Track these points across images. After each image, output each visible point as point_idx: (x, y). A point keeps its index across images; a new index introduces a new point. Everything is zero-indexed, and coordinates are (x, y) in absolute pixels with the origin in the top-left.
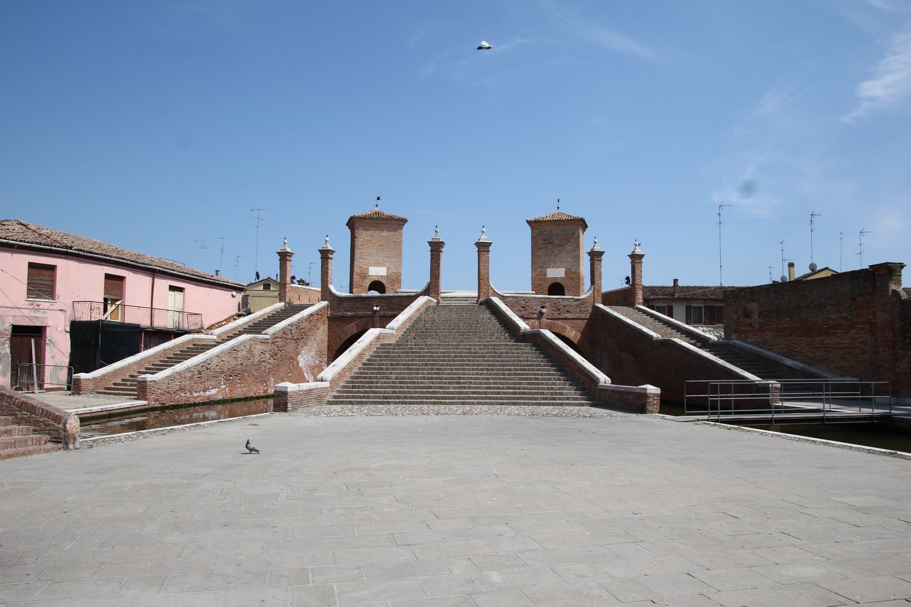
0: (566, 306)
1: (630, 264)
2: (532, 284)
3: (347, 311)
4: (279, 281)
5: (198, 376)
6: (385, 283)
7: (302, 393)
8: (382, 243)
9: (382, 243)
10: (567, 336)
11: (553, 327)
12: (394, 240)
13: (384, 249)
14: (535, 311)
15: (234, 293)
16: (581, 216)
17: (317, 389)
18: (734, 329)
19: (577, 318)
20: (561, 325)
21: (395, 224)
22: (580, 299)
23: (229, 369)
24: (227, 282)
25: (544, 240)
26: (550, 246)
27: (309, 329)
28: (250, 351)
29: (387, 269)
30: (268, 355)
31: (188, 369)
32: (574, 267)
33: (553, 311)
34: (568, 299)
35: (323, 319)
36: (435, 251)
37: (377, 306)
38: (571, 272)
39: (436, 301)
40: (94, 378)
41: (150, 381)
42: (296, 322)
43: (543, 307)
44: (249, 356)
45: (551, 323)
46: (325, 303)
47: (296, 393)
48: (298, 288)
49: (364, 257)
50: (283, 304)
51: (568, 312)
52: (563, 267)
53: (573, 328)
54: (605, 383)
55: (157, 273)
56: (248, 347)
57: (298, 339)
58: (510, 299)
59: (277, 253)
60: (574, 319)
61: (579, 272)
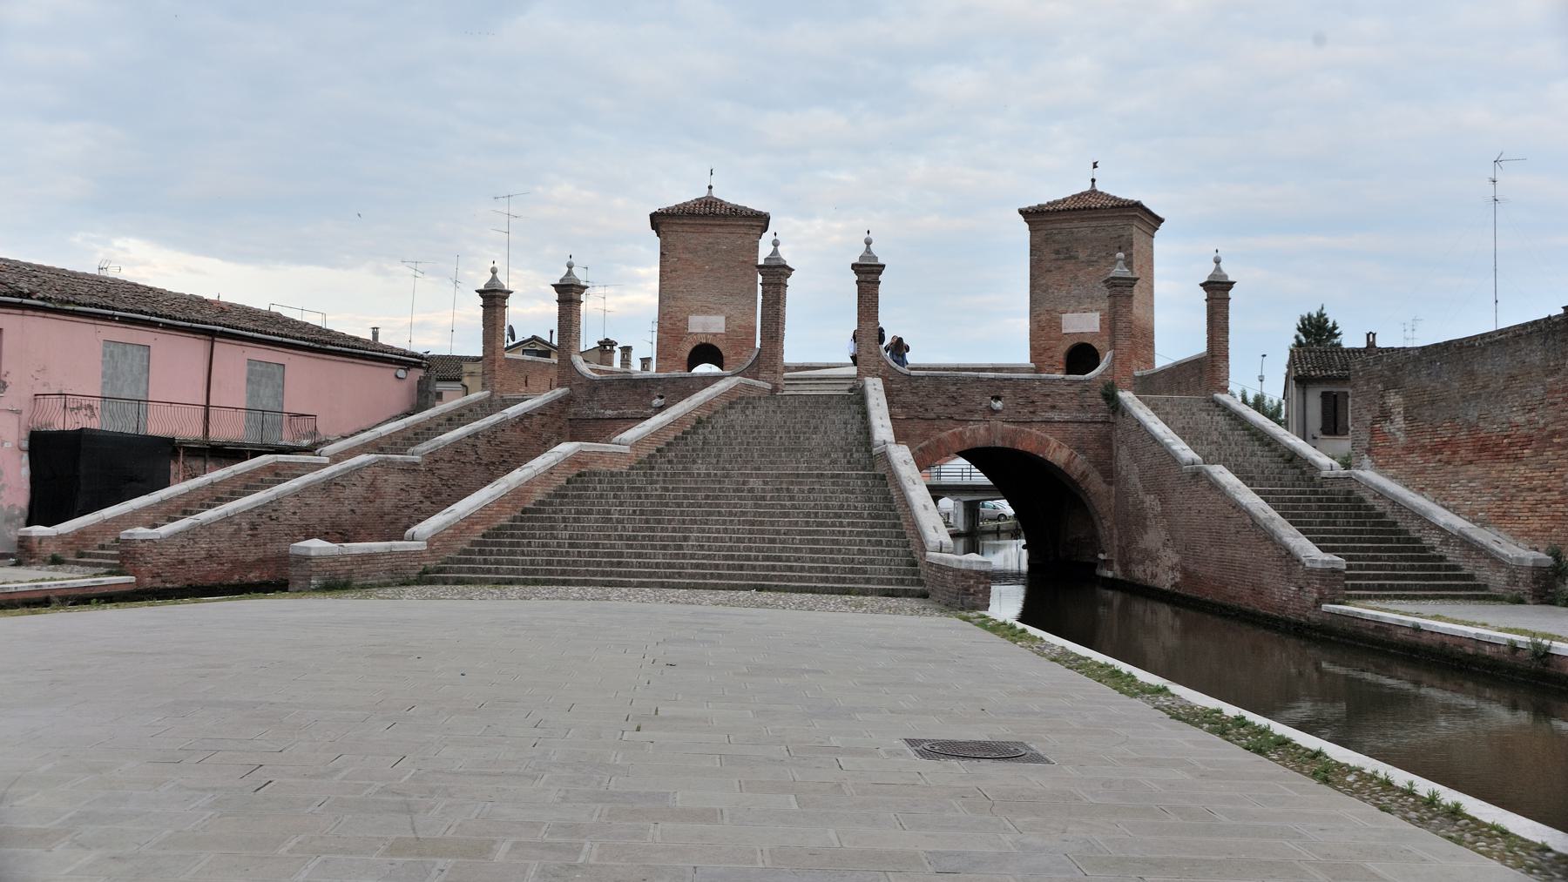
0: (1048, 395)
1: (1206, 303)
2: (1032, 348)
3: (604, 407)
4: (555, 342)
5: (249, 532)
6: (721, 348)
7: (349, 559)
8: (716, 265)
9: (716, 265)
10: (1049, 458)
12: (741, 259)
13: (720, 278)
15: (401, 373)
16: (1136, 200)
17: (391, 553)
18: (1367, 446)
19: (1075, 420)
20: (1037, 436)
21: (743, 225)
23: (322, 520)
24: (383, 352)
25: (1057, 252)
26: (1069, 266)
27: (522, 444)
28: (372, 486)
30: (417, 496)
31: (228, 519)
33: (1020, 407)
34: (1054, 380)
35: (558, 424)
37: (661, 397)
40: (59, 536)
41: (143, 541)
42: (488, 430)
43: (997, 398)
44: (372, 496)
46: (559, 392)
47: (334, 558)
48: (523, 361)
49: (680, 295)
50: (487, 393)
51: (1053, 407)
52: (1097, 310)
53: (1064, 442)
54: (941, 551)
55: (220, 337)
56: (368, 478)
57: (494, 463)
59: (477, 291)
60: (1067, 422)
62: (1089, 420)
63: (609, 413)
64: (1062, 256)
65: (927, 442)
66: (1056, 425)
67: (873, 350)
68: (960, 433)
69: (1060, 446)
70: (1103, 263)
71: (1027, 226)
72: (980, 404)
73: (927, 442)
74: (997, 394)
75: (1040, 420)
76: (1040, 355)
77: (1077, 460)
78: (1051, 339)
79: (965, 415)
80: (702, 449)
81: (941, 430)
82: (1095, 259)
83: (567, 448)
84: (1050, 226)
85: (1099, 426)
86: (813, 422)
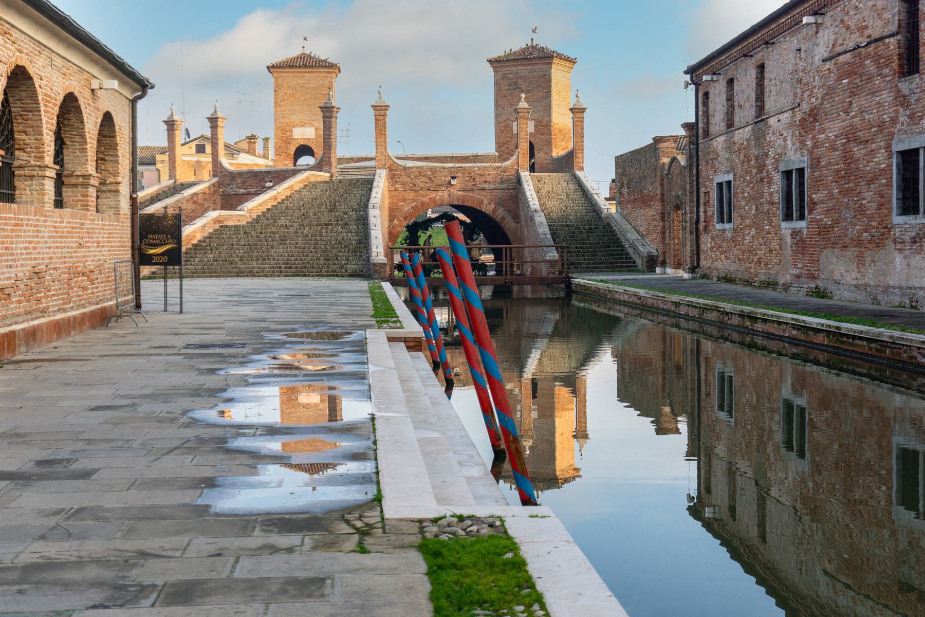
2: (497, 143)
3: (240, 188)
8: (309, 96)
9: (309, 96)
10: (483, 210)
25: (510, 85)
29: (316, 129)
32: (546, 119)
36: (327, 117)
37: (271, 182)
38: (543, 126)
39: (328, 175)
43: (453, 178)
45: (464, 196)
58: (413, 170)
61: (550, 126)
63: (242, 191)
64: (512, 87)
68: (434, 197)
69: (490, 203)
70: (535, 91)
71: (492, 69)
76: (501, 147)
77: (499, 210)
78: (506, 137)
80: (285, 212)
82: (530, 88)
83: (213, 214)
84: (505, 69)
85: (512, 191)
86: (345, 195)
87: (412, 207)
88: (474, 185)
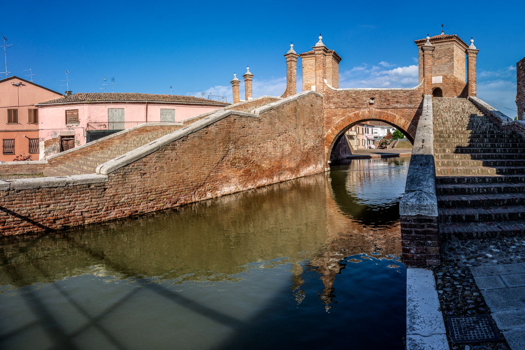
11: (382, 116)
14: (366, 102)
19: (407, 107)
20: (390, 114)
22: (408, 91)
43: (373, 99)
45: (381, 112)
51: (397, 102)
53: (403, 117)
62: (413, 107)
65: (344, 118)
66: (398, 109)
67: (321, 81)
68: (358, 113)
72: (366, 101)
73: (344, 118)
74: (373, 97)
75: (391, 107)
79: (359, 106)
81: (350, 113)
87: (342, 120)
88: (389, 104)
